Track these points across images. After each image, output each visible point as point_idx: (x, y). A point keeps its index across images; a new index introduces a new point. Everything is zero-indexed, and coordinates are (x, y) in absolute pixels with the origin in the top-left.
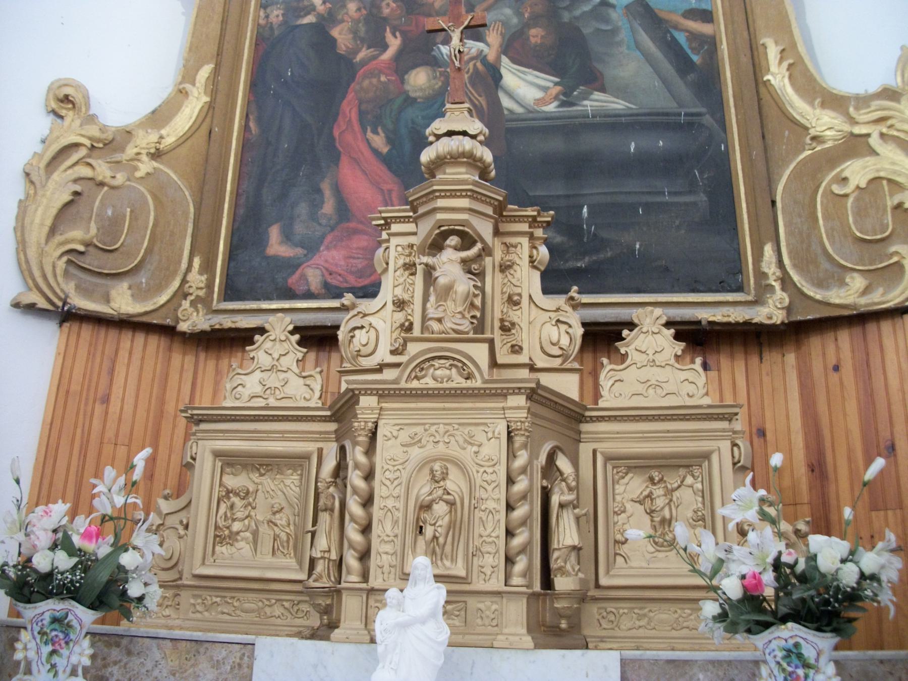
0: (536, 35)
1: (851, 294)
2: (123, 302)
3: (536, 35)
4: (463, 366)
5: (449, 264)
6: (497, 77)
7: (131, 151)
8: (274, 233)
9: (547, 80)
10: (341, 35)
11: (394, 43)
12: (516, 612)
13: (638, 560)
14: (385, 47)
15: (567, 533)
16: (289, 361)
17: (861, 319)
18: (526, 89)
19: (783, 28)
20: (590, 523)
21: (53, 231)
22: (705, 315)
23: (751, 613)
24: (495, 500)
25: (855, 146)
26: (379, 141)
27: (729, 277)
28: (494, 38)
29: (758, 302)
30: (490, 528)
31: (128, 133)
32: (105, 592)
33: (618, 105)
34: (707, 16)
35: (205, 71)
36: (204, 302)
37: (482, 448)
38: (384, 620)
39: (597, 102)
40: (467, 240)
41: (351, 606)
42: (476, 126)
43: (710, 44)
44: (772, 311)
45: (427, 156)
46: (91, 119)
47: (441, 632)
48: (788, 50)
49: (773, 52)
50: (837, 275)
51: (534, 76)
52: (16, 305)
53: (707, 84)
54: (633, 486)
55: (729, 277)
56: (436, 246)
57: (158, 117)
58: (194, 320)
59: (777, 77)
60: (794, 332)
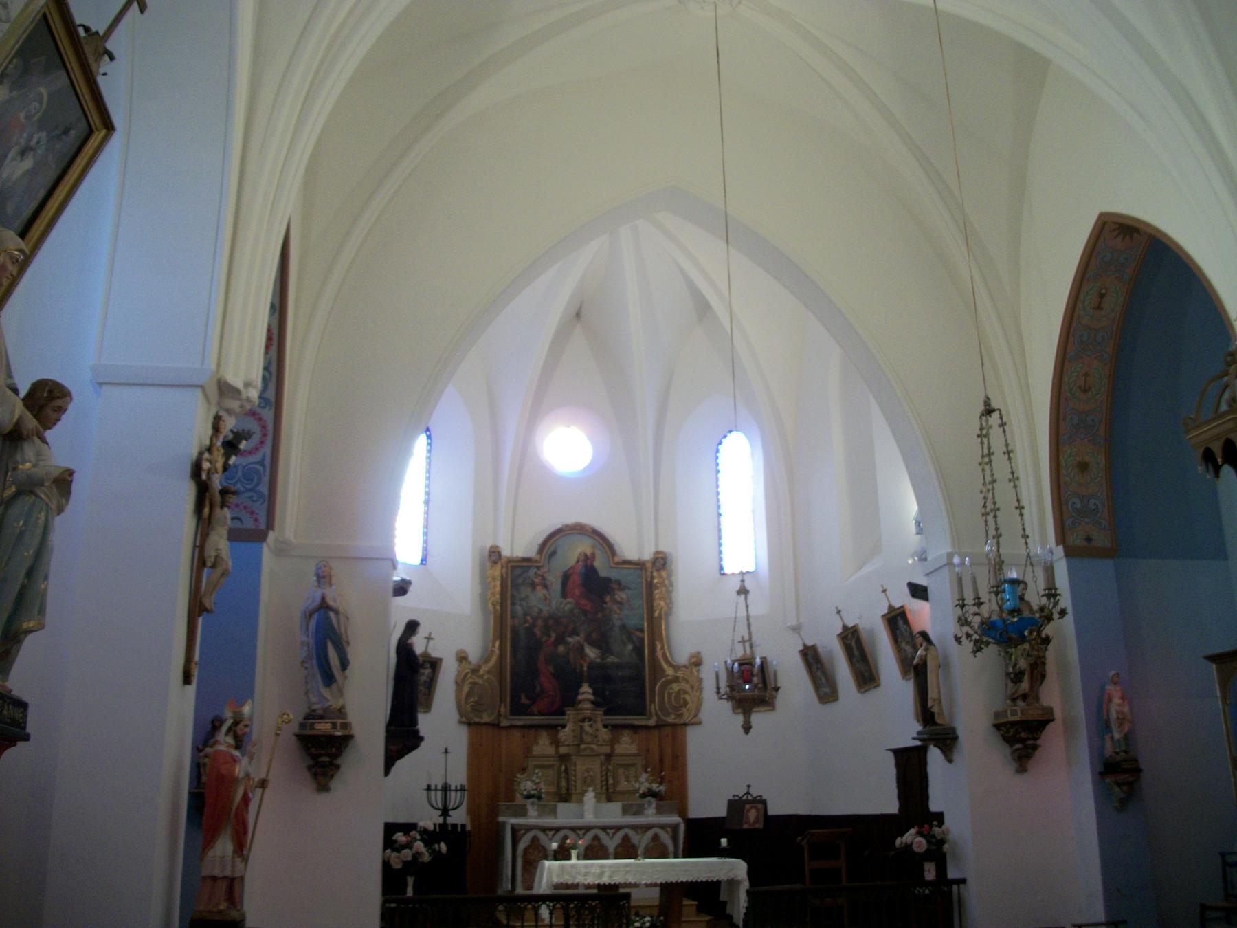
0: (594, 636)
1: (671, 719)
2: (486, 718)
3: (594, 636)
4: (592, 750)
5: (586, 725)
6: (582, 649)
7: (482, 672)
8: (523, 696)
9: (597, 651)
10: (537, 631)
11: (553, 636)
12: (604, 797)
13: (624, 785)
14: (549, 636)
15: (611, 781)
16: (547, 743)
17: (674, 725)
18: (591, 653)
19: (661, 640)
20: (614, 778)
21: (466, 699)
22: (636, 723)
23: (644, 796)
24: (598, 776)
25: (676, 680)
26: (551, 669)
27: (641, 711)
28: (582, 635)
29: (649, 719)
30: (598, 781)
31: (479, 667)
32: (539, 798)
33: (616, 660)
34: (642, 630)
35: (497, 643)
36: (505, 717)
37: (596, 766)
38: (585, 798)
39: (611, 659)
40: (590, 720)
41: (574, 797)
42: (590, 691)
43: (642, 640)
44: (652, 722)
45: (580, 697)
46: (470, 663)
47: (594, 800)
48: (662, 648)
49: (659, 646)
50: (668, 714)
51: (595, 650)
52: (461, 722)
53: (639, 650)
54: (621, 771)
55: (641, 711)
56: (583, 721)
57: (487, 660)
58: (505, 723)
59: (659, 654)
60: (658, 726)
